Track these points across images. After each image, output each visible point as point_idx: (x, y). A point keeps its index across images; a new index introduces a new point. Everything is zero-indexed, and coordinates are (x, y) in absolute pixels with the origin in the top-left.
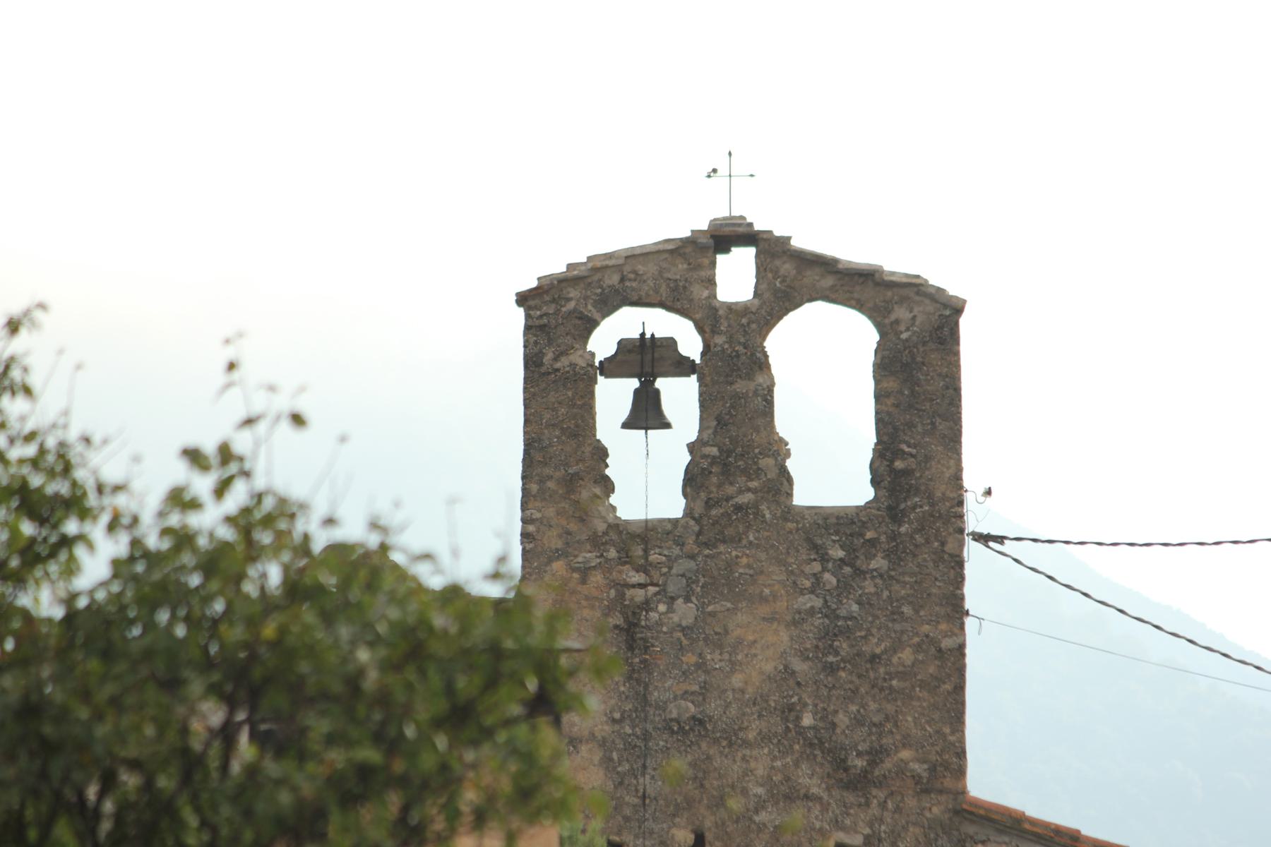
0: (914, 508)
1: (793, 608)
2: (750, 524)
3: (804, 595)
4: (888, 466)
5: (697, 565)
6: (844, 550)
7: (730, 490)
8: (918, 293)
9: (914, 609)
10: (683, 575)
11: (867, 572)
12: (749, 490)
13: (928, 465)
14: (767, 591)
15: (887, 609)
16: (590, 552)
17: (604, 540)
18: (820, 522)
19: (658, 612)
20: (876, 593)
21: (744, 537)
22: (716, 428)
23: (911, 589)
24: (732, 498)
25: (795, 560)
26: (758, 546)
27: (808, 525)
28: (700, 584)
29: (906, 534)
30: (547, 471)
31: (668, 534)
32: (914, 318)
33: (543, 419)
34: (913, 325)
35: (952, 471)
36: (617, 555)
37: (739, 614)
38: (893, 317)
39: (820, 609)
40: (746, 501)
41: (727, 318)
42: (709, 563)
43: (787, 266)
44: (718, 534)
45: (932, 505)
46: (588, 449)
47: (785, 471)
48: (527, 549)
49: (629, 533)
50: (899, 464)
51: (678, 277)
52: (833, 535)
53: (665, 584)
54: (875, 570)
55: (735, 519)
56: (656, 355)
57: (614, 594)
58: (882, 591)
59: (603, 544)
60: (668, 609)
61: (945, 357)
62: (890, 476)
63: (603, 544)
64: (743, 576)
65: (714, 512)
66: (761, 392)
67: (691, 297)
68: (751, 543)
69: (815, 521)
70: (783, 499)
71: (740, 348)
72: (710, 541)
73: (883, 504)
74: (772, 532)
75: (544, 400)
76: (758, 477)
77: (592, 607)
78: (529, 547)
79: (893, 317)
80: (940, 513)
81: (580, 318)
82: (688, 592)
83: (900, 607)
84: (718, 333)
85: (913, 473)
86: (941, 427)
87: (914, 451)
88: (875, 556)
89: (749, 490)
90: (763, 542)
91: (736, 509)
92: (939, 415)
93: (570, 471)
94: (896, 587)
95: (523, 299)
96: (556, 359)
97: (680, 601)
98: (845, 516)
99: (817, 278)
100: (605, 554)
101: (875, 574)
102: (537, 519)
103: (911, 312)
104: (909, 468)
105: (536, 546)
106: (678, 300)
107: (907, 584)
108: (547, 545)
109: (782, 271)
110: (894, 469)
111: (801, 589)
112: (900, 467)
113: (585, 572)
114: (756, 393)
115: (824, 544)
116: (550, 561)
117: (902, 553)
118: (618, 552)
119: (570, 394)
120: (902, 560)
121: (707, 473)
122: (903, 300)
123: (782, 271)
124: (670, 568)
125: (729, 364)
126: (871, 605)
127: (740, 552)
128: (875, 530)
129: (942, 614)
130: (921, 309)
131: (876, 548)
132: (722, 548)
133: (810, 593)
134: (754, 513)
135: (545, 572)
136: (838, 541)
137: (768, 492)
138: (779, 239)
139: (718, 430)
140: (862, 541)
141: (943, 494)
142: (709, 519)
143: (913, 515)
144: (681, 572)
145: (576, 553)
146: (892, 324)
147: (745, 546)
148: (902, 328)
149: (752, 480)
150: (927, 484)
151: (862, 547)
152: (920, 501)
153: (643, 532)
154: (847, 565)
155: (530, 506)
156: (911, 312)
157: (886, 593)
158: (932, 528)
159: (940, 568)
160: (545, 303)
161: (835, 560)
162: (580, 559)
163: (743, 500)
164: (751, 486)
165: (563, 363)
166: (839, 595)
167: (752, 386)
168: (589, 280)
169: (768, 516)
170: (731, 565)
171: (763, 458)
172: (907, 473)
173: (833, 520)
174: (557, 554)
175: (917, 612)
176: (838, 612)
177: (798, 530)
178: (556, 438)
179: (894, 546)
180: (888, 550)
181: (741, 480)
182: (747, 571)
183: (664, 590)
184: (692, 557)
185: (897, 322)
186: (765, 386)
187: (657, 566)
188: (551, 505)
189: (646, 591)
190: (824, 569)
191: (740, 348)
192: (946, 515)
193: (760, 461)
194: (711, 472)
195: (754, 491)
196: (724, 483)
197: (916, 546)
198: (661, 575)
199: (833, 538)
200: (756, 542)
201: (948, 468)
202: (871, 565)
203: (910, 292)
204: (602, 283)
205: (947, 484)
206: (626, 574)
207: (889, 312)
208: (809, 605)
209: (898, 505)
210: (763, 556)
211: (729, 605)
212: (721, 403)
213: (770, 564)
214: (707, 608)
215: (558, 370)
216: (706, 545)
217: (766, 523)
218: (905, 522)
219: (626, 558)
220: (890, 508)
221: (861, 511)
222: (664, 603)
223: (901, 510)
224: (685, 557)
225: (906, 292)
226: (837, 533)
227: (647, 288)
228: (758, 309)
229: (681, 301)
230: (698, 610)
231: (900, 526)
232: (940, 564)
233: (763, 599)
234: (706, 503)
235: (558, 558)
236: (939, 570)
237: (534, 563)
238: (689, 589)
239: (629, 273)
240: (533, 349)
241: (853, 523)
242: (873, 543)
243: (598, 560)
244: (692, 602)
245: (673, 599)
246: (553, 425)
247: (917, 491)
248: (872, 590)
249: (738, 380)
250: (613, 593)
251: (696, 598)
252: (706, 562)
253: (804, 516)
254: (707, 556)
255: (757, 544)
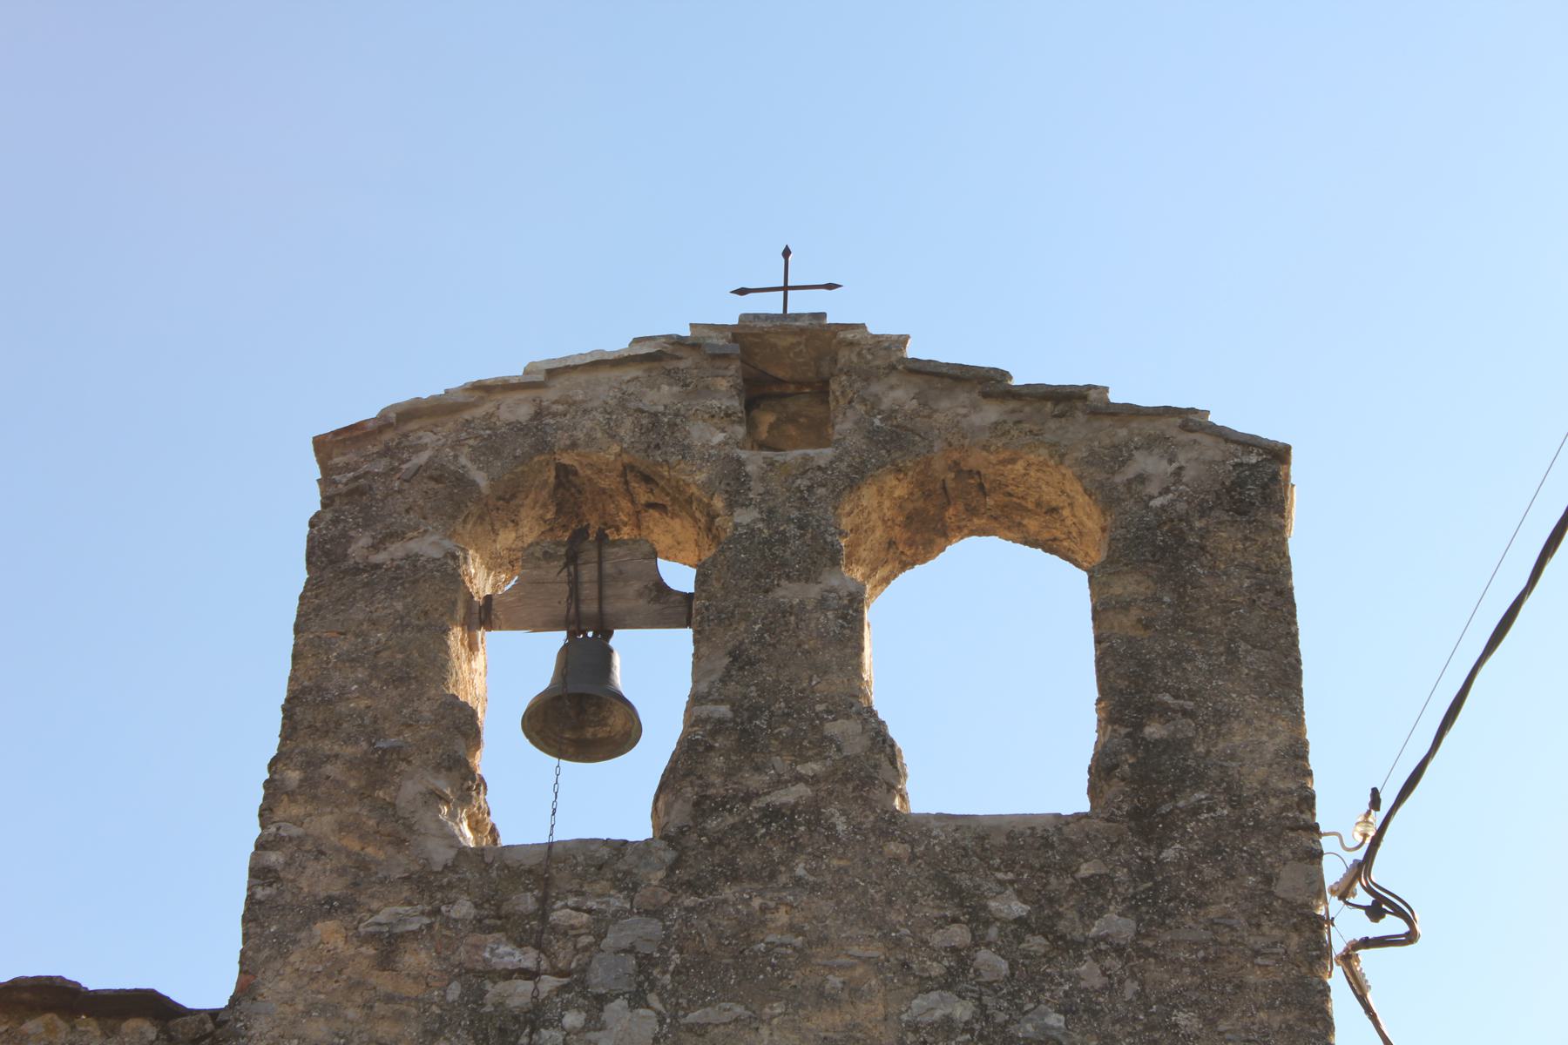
0: (1195, 811)
1: (900, 1021)
2: (797, 844)
3: (928, 991)
4: (1128, 735)
5: (665, 928)
6: (1025, 902)
7: (754, 781)
8: (1185, 427)
9: (1203, 1017)
10: (631, 950)
11: (1084, 944)
12: (799, 778)
13: (1224, 730)
14: (835, 981)
15: (1135, 1019)
16: (410, 903)
17: (445, 880)
18: (969, 843)
19: (563, 1029)
20: (1108, 988)
21: (783, 869)
22: (728, 669)
23: (1193, 974)
24: (758, 795)
25: (907, 919)
26: (814, 888)
27: (938, 849)
28: (671, 968)
29: (1177, 864)
30: (326, 746)
31: (600, 868)
32: (1179, 472)
33: (333, 650)
34: (1178, 482)
35: (1282, 740)
36: (473, 911)
37: (765, 1031)
38: (1131, 471)
39: (966, 1023)
40: (791, 799)
41: (762, 479)
42: (694, 922)
43: (899, 394)
44: (720, 866)
45: (1237, 802)
46: (426, 709)
47: (884, 741)
48: (258, 896)
49: (507, 867)
50: (1154, 730)
51: (661, 408)
52: (998, 870)
53: (584, 969)
54: (1104, 939)
55: (763, 836)
56: (608, 567)
57: (458, 992)
58: (1121, 982)
59: (441, 888)
60: (588, 1021)
61: (1252, 536)
62: (1134, 755)
63: (441, 888)
64: (778, 950)
65: (712, 824)
66: (834, 603)
67: (686, 442)
68: (798, 881)
69: (955, 841)
70: (878, 794)
71: (792, 530)
72: (699, 878)
73: (1119, 808)
74: (851, 859)
75: (341, 617)
76: (820, 756)
77: (400, 1016)
78: (261, 893)
79: (1131, 471)
80: (1257, 822)
81: (437, 480)
82: (640, 984)
83: (1169, 1015)
84: (743, 505)
85: (1190, 745)
86: (1249, 659)
87: (1190, 705)
88: (1102, 910)
89: (799, 778)
90: (828, 878)
91: (765, 816)
92: (1244, 638)
93: (381, 744)
94: (1155, 972)
95: (325, 446)
96: (376, 547)
97: (620, 1004)
98: (1029, 832)
99: (963, 411)
100: (444, 909)
101: (1103, 946)
102: (291, 839)
103: (1171, 461)
104: (1179, 736)
105: (280, 893)
106: (657, 447)
107: (1183, 965)
108: (306, 890)
109: (886, 404)
110: (1143, 739)
111: (921, 978)
112: (1157, 736)
113: (389, 946)
114: (822, 604)
115: (978, 887)
116: (310, 919)
117: (1169, 901)
118: (476, 906)
119: (399, 606)
120: (1170, 915)
121: (701, 749)
122: (1150, 443)
123: (886, 404)
124: (601, 936)
125: (763, 557)
126: (1095, 1014)
127: (771, 899)
128: (1102, 857)
129: (1275, 1026)
130: (1194, 454)
131: (1104, 896)
132: (728, 892)
133: (941, 988)
134: (808, 823)
135: (295, 942)
136: (1012, 882)
137: (847, 778)
138: (879, 340)
139: (734, 673)
140: (1069, 881)
141: (1264, 784)
142: (700, 836)
143: (1193, 824)
144: (625, 944)
145: (375, 905)
146: (1129, 482)
147: (785, 887)
148: (1153, 489)
149: (807, 760)
150: (1221, 766)
151: (1070, 893)
152: (1206, 799)
153: (540, 864)
154: (1033, 932)
155: (280, 813)
156: (1171, 461)
157: (1131, 988)
158: (1241, 851)
159: (1265, 929)
160: (368, 458)
161: (1005, 922)
162: (381, 918)
163: (784, 799)
164: (803, 772)
165: (396, 551)
166: (1014, 995)
167: (814, 591)
168: (467, 415)
169: (841, 827)
170: (748, 926)
171: (835, 720)
172: (1172, 746)
173: (1001, 840)
174: (327, 907)
175: (1211, 1023)
176: (1012, 1029)
177: (913, 858)
178: (356, 683)
179: (1150, 889)
180: (1133, 897)
181: (781, 763)
182: (788, 938)
183: (583, 983)
184: (656, 913)
185: (1142, 479)
186: (843, 593)
187: (565, 932)
188: (329, 810)
189: (536, 984)
190: (978, 942)
191: (792, 530)
192: (1273, 825)
193: (827, 725)
194: (710, 748)
195: (813, 781)
196: (740, 769)
197: (1203, 885)
198: (577, 951)
199: (1000, 875)
200: (812, 879)
201: (1272, 735)
202: (1094, 930)
203: (1170, 427)
204: (493, 420)
205: (1270, 765)
206: (492, 950)
207: (1123, 463)
208: (938, 1014)
209: (1155, 807)
210: (827, 907)
211: (739, 1010)
212: (742, 626)
213: (845, 921)
214: (685, 1016)
215: (377, 566)
216: (692, 887)
217: (838, 840)
218: (1175, 839)
219: (495, 919)
220: (1136, 814)
221: (1067, 823)
222: (579, 1008)
223: (1162, 816)
224: (638, 913)
225: (1160, 425)
226: (1009, 866)
227: (589, 424)
228: (831, 462)
229: (664, 449)
230: (661, 1022)
231: (1161, 847)
232: (1264, 919)
233: (824, 998)
234: (696, 804)
235: (328, 915)
236: (1263, 935)
237: (269, 927)
238: (642, 978)
239: (554, 403)
240: (327, 528)
241: (1048, 845)
242: (1096, 885)
243: (426, 921)
244: (648, 1007)
245: (601, 1000)
246: (353, 660)
247: (1199, 781)
248: (1097, 981)
249: (784, 582)
250: (454, 991)
251: (659, 995)
252: (686, 921)
253: (930, 830)
254: (689, 910)
255: (815, 883)
